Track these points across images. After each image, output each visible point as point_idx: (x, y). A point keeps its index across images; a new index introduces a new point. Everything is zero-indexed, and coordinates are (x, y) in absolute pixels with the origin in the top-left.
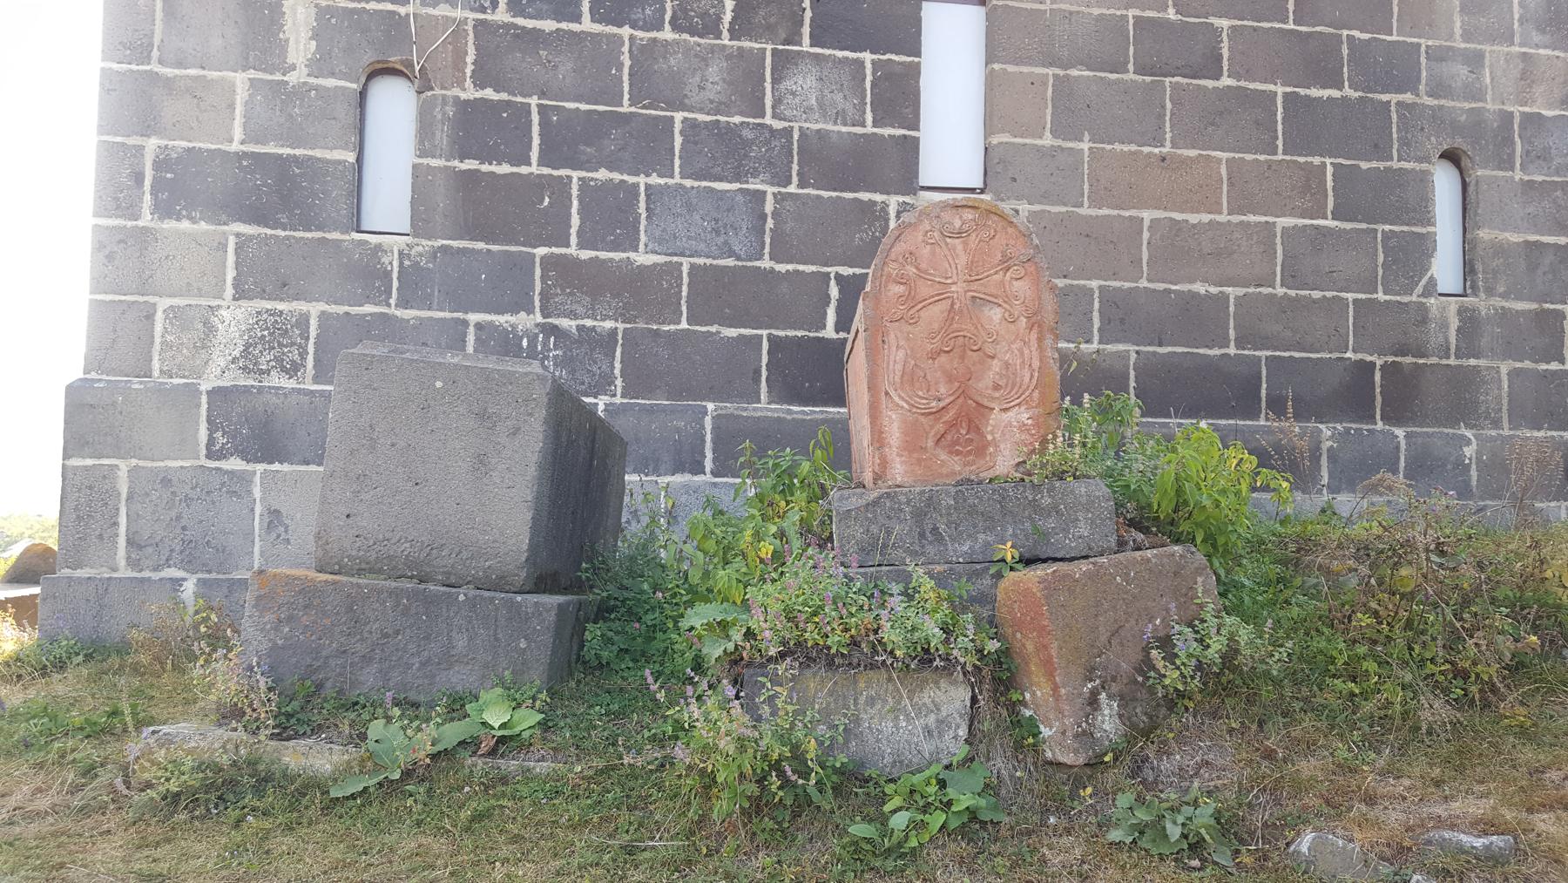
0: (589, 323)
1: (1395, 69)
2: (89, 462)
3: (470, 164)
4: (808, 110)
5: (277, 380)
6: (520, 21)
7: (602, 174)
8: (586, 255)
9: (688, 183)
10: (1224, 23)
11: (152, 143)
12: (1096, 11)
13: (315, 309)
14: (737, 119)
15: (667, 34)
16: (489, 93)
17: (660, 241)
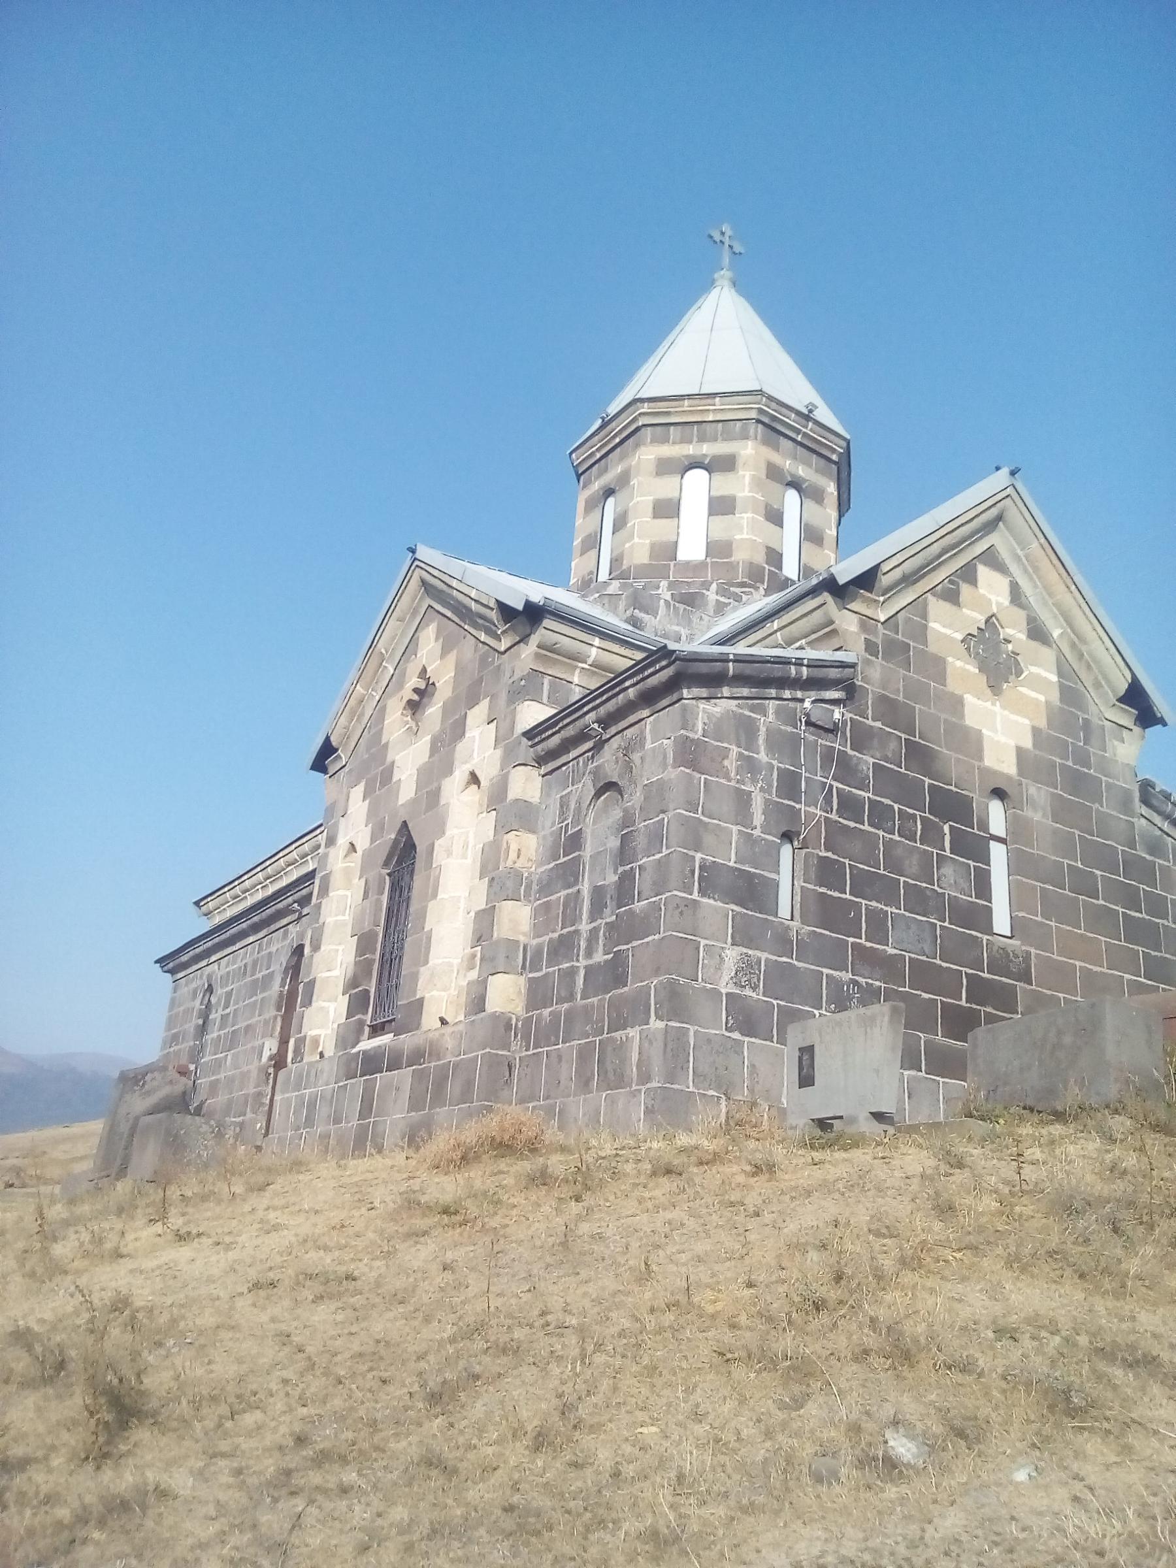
0: (870, 981)
1: (1157, 907)
2: (678, 1025)
3: (823, 890)
4: (950, 885)
5: (748, 992)
6: (841, 820)
7: (874, 904)
8: (869, 944)
9: (907, 914)
10: (1098, 873)
11: (699, 856)
12: (1054, 858)
13: (764, 956)
14: (924, 885)
15: (896, 837)
16: (829, 854)
17: (897, 943)
